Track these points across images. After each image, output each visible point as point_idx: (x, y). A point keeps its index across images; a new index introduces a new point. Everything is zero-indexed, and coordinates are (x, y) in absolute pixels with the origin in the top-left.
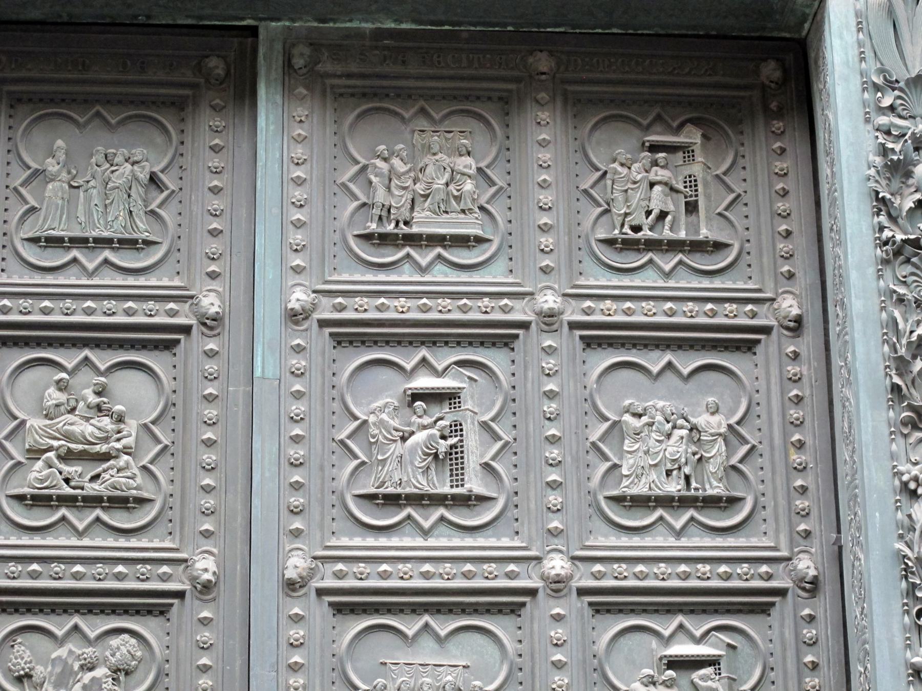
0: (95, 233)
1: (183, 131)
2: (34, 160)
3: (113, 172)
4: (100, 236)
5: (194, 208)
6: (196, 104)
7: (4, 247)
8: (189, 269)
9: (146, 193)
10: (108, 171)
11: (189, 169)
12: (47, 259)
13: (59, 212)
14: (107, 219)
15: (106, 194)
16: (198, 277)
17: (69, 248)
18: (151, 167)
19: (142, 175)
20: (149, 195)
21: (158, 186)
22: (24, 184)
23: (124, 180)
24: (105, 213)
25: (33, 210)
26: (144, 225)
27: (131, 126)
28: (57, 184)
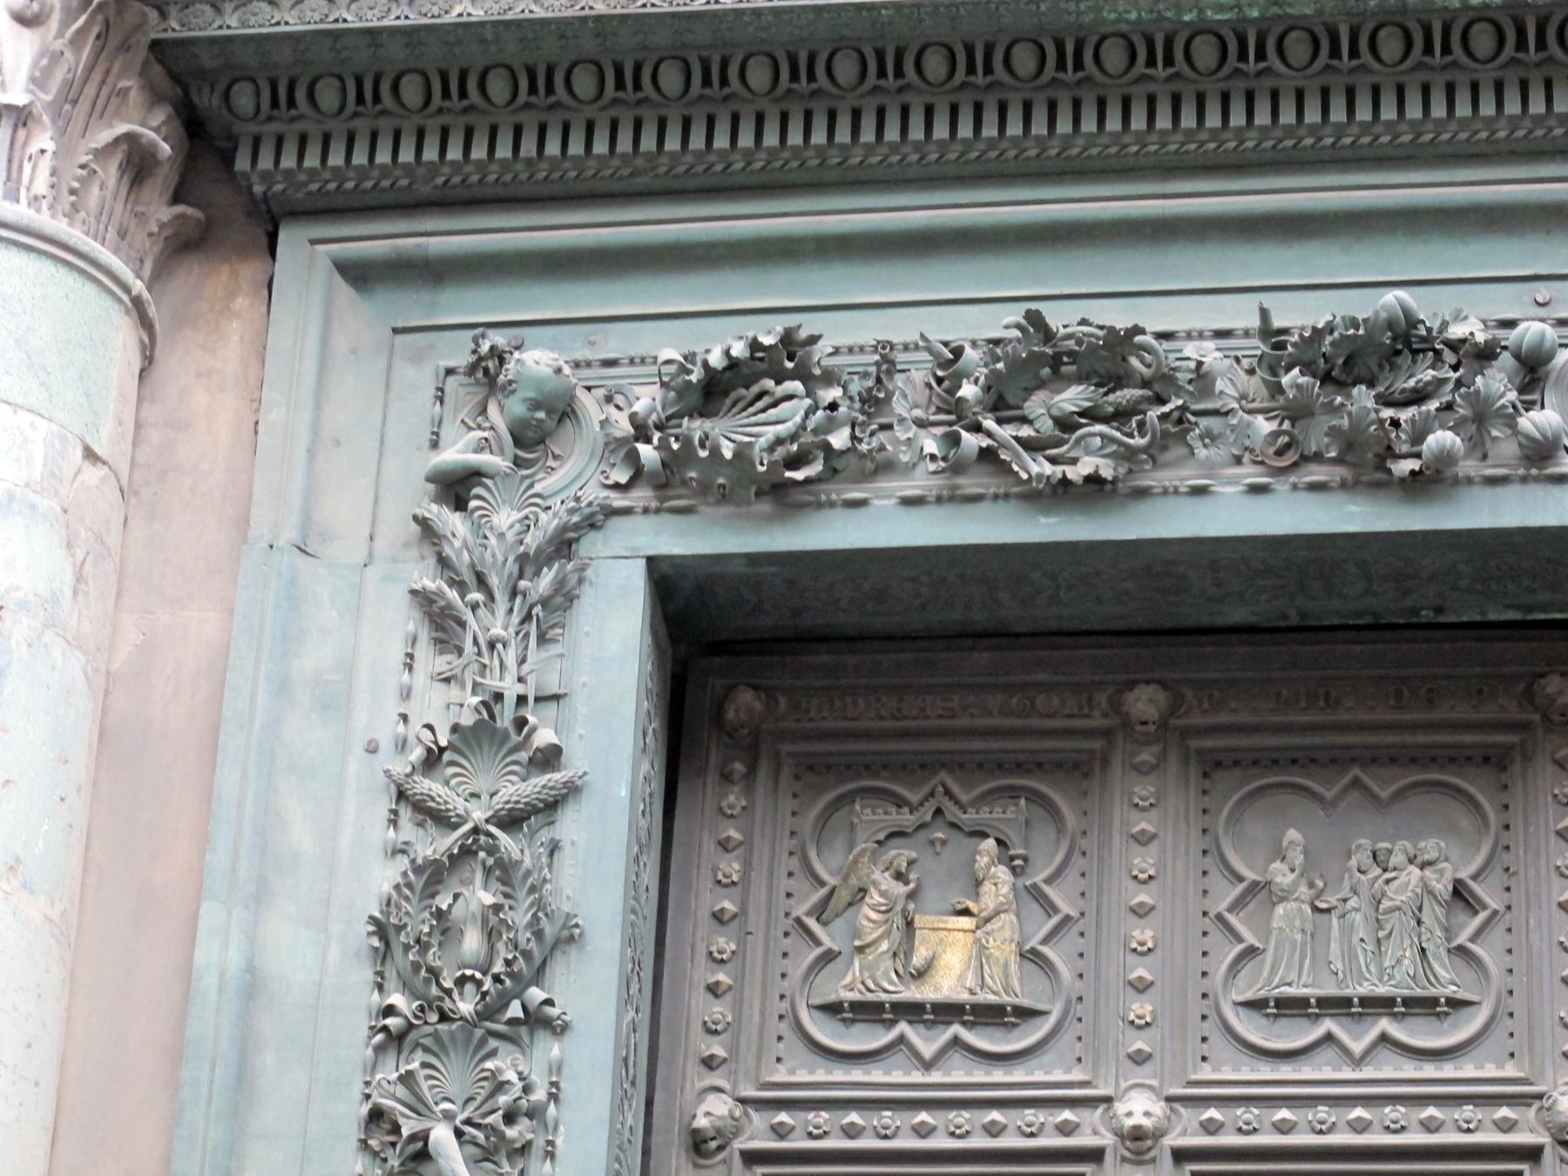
0: (1364, 990)
1: (1506, 807)
2: (1251, 868)
3: (1388, 881)
4: (1371, 994)
5: (1535, 939)
6: (1527, 758)
7: (1204, 1017)
8: (1531, 1049)
9: (1447, 916)
10: (1380, 881)
11: (1522, 873)
12: (1279, 1037)
13: (1297, 954)
14: (1381, 963)
15: (1378, 921)
16: (1548, 1061)
17: (1318, 1016)
18: (1455, 870)
19: (1440, 886)
20: (1453, 921)
21: (1468, 903)
22: (1234, 907)
23: (1409, 894)
24: (1379, 953)
25: (1251, 952)
26: (1448, 972)
27: (1417, 801)
28: (1292, 905)
